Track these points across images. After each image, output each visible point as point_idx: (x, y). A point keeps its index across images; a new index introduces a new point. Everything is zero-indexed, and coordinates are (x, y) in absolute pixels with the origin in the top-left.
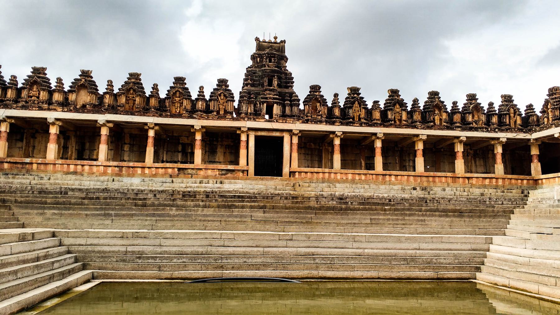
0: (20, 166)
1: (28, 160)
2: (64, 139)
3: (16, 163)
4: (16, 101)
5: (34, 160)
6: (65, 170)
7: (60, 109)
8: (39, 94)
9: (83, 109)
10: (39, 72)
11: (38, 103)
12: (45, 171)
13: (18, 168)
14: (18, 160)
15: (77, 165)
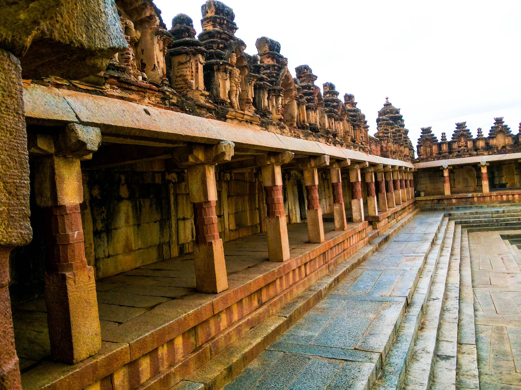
0: (464, 200)
1: (470, 195)
2: (476, 170)
3: (461, 198)
4: (450, 153)
5: (475, 194)
6: (499, 200)
7: (486, 153)
8: (467, 143)
9: (503, 150)
10: (461, 126)
11: (468, 151)
12: (485, 202)
13: (463, 201)
14: (461, 195)
15: (508, 195)
